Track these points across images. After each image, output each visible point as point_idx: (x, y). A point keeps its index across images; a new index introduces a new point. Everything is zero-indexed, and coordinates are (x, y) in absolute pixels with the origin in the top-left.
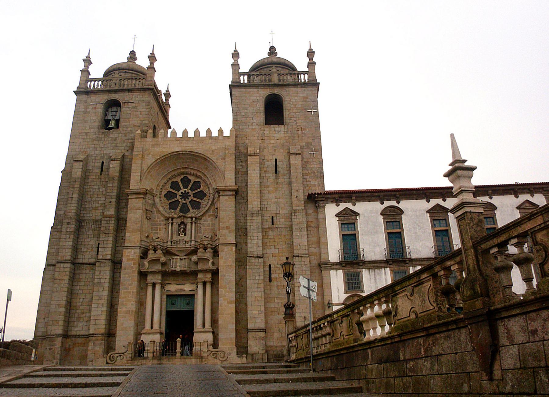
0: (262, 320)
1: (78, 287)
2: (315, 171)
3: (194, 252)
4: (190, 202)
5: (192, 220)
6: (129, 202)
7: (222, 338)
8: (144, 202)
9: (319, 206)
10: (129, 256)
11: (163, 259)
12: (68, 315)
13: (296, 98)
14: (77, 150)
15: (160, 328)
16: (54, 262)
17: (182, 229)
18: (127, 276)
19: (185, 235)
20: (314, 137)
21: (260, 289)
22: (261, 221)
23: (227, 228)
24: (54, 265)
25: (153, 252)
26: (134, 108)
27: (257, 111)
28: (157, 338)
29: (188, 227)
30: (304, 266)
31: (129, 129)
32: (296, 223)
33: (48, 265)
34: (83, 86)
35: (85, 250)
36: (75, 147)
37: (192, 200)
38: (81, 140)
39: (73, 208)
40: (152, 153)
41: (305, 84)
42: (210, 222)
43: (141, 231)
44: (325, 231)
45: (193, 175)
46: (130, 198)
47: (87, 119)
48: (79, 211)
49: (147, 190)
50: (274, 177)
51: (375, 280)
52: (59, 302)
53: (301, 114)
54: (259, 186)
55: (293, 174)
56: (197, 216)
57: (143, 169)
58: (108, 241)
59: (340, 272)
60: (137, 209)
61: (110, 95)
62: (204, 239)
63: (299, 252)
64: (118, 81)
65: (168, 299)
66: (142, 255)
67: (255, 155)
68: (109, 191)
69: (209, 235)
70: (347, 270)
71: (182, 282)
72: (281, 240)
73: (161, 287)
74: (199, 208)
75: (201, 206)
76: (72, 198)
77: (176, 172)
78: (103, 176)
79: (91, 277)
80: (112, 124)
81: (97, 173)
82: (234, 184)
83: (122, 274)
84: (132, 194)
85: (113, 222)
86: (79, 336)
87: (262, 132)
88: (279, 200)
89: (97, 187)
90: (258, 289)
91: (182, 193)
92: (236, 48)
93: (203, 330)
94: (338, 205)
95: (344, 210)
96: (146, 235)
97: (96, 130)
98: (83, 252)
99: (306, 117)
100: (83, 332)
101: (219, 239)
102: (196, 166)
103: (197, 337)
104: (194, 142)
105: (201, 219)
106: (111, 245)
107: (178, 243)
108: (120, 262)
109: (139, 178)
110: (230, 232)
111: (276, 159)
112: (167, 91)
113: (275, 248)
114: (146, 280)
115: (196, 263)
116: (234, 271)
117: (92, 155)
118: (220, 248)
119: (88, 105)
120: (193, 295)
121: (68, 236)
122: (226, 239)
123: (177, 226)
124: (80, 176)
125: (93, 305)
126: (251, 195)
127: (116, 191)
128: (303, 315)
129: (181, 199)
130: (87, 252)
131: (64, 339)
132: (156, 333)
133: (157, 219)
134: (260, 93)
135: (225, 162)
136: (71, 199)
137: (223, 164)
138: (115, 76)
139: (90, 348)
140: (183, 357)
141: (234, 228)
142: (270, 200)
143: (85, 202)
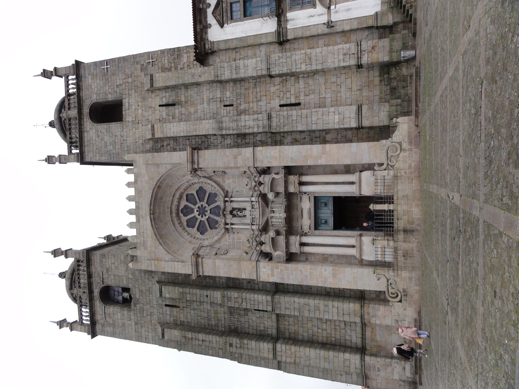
0: (346, 110)
1: (305, 334)
2: (172, 58)
3: (264, 197)
4: (209, 206)
5: (227, 201)
6: (207, 274)
7: (368, 159)
8: (207, 257)
9: (211, 49)
10: (268, 274)
11: (272, 233)
12: (338, 347)
13: (93, 87)
14: (154, 334)
15: (354, 237)
16: (276, 362)
17: (239, 212)
18: (291, 277)
19: (245, 209)
20: (134, 62)
21: (308, 114)
23: (235, 157)
24: (279, 363)
25: (264, 245)
26: (108, 270)
27: (108, 131)
28: (367, 239)
29: (235, 205)
31: (130, 276)
32: (230, 74)
33: (279, 368)
34: (87, 328)
35: (262, 325)
36: (150, 337)
37: (207, 203)
38: (143, 329)
39: (214, 339)
40: (153, 249)
41: (78, 78)
42: (230, 181)
43: (239, 260)
44: (240, 39)
45: (179, 202)
46: (203, 273)
47: (121, 325)
48: (218, 332)
49: (193, 254)
50: (180, 106)
52: (321, 358)
53: (110, 79)
55: (174, 83)
56: (223, 195)
57: (171, 260)
58: (251, 299)
59: (290, 15)
60: (215, 266)
61: (95, 298)
62: (249, 186)
63: (264, 67)
64: (81, 290)
65: (320, 228)
66: (267, 259)
68: (195, 299)
69: (246, 180)
70: (288, 8)
71: (300, 212)
72: (251, 94)
73: (305, 236)
74: (216, 195)
75: (213, 192)
76: (203, 341)
77: (176, 222)
78: (181, 305)
79: (292, 319)
80: (126, 295)
81: (177, 312)
82: (185, 152)
83: (289, 283)
84: (198, 272)
85: (229, 293)
86: (363, 335)
87: (130, 124)
88: (205, 100)
89: (192, 312)
90: (308, 116)
91: (199, 215)
92: (43, 160)
93: (358, 184)
95: (215, 17)
96: (245, 254)
97: (132, 313)
98: (264, 328)
99: (113, 75)
100: (359, 329)
101: (249, 167)
102: (168, 198)
103: (367, 191)
104: (141, 201)
105: (227, 191)
106: (256, 296)
107: (253, 217)
108: (276, 284)
109: (180, 263)
110: (240, 154)
111: (160, 106)
112: (105, 238)
113: (261, 101)
114: (296, 254)
115: (277, 194)
117: (158, 318)
118: (259, 165)
119: (105, 323)
120: (316, 198)
121: (246, 346)
122: (248, 159)
123: (235, 219)
124: (179, 332)
125: (326, 317)
126: (197, 132)
127: (195, 291)
128: (341, 57)
129: (205, 215)
130: (264, 324)
131: (367, 352)
132: (361, 242)
133: (227, 243)
134: (88, 129)
135: (162, 164)
136: (204, 343)
137: (164, 166)
138: (76, 293)
139: (378, 322)
140: (395, 202)
141: (235, 150)
142: (205, 110)
143: (209, 325)
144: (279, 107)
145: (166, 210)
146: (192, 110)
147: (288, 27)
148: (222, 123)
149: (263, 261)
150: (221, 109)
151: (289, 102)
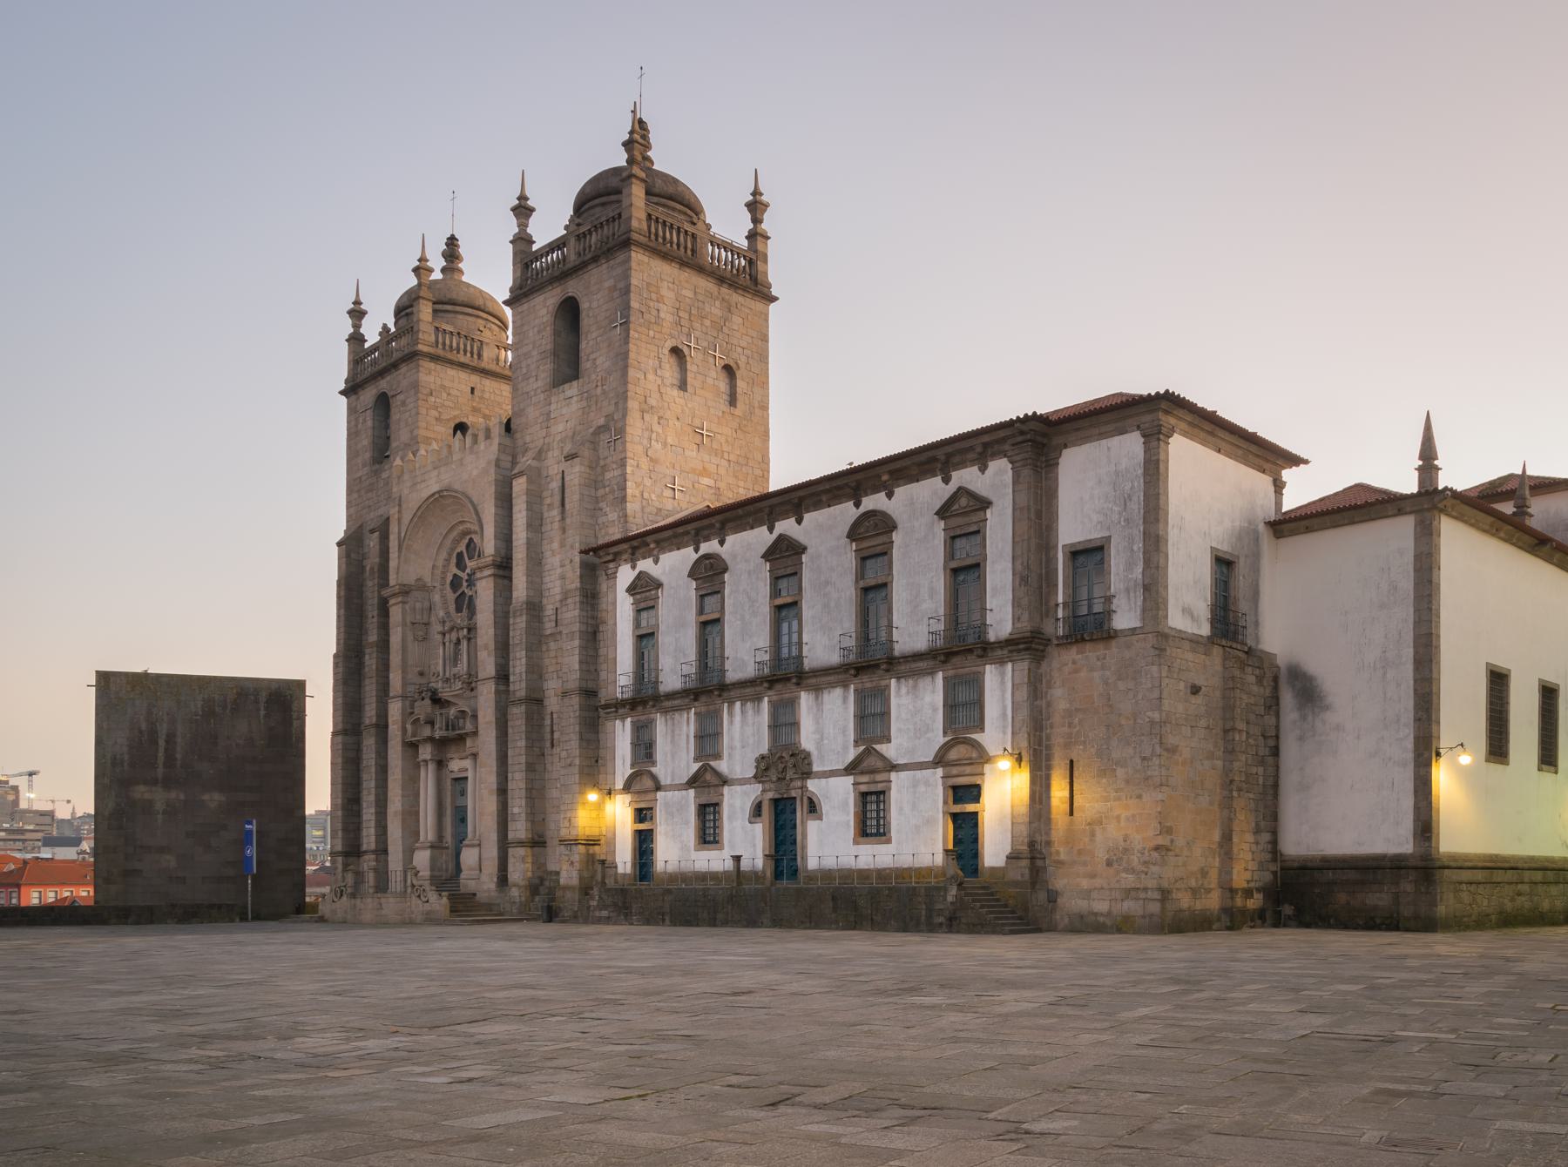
10: (393, 715)
22: (524, 625)
23: (486, 647)
30: (572, 714)
49: (405, 585)
51: (673, 737)
54: (525, 546)
67: (521, 474)
77: (455, 533)
85: (375, 655)
91: (468, 574)
94: (634, 567)
106: (375, 698)
107: (452, 681)
111: (563, 471)
116: (494, 734)
127: (376, 594)
140: (376, 894)
141: (492, 646)
144: (550, 712)
145: (459, 514)
146: (555, 545)
147: (617, 721)
148: (521, 615)
149: (407, 703)
150: (553, 604)
151: (554, 729)
